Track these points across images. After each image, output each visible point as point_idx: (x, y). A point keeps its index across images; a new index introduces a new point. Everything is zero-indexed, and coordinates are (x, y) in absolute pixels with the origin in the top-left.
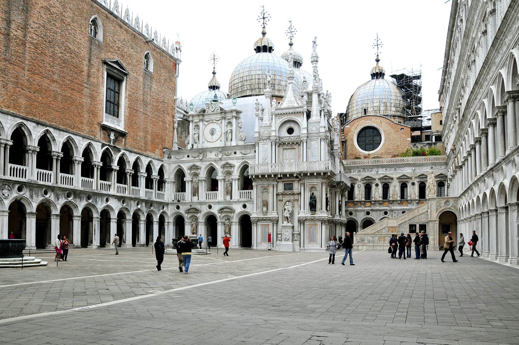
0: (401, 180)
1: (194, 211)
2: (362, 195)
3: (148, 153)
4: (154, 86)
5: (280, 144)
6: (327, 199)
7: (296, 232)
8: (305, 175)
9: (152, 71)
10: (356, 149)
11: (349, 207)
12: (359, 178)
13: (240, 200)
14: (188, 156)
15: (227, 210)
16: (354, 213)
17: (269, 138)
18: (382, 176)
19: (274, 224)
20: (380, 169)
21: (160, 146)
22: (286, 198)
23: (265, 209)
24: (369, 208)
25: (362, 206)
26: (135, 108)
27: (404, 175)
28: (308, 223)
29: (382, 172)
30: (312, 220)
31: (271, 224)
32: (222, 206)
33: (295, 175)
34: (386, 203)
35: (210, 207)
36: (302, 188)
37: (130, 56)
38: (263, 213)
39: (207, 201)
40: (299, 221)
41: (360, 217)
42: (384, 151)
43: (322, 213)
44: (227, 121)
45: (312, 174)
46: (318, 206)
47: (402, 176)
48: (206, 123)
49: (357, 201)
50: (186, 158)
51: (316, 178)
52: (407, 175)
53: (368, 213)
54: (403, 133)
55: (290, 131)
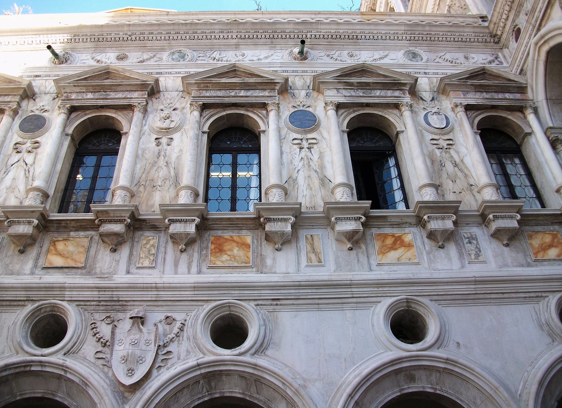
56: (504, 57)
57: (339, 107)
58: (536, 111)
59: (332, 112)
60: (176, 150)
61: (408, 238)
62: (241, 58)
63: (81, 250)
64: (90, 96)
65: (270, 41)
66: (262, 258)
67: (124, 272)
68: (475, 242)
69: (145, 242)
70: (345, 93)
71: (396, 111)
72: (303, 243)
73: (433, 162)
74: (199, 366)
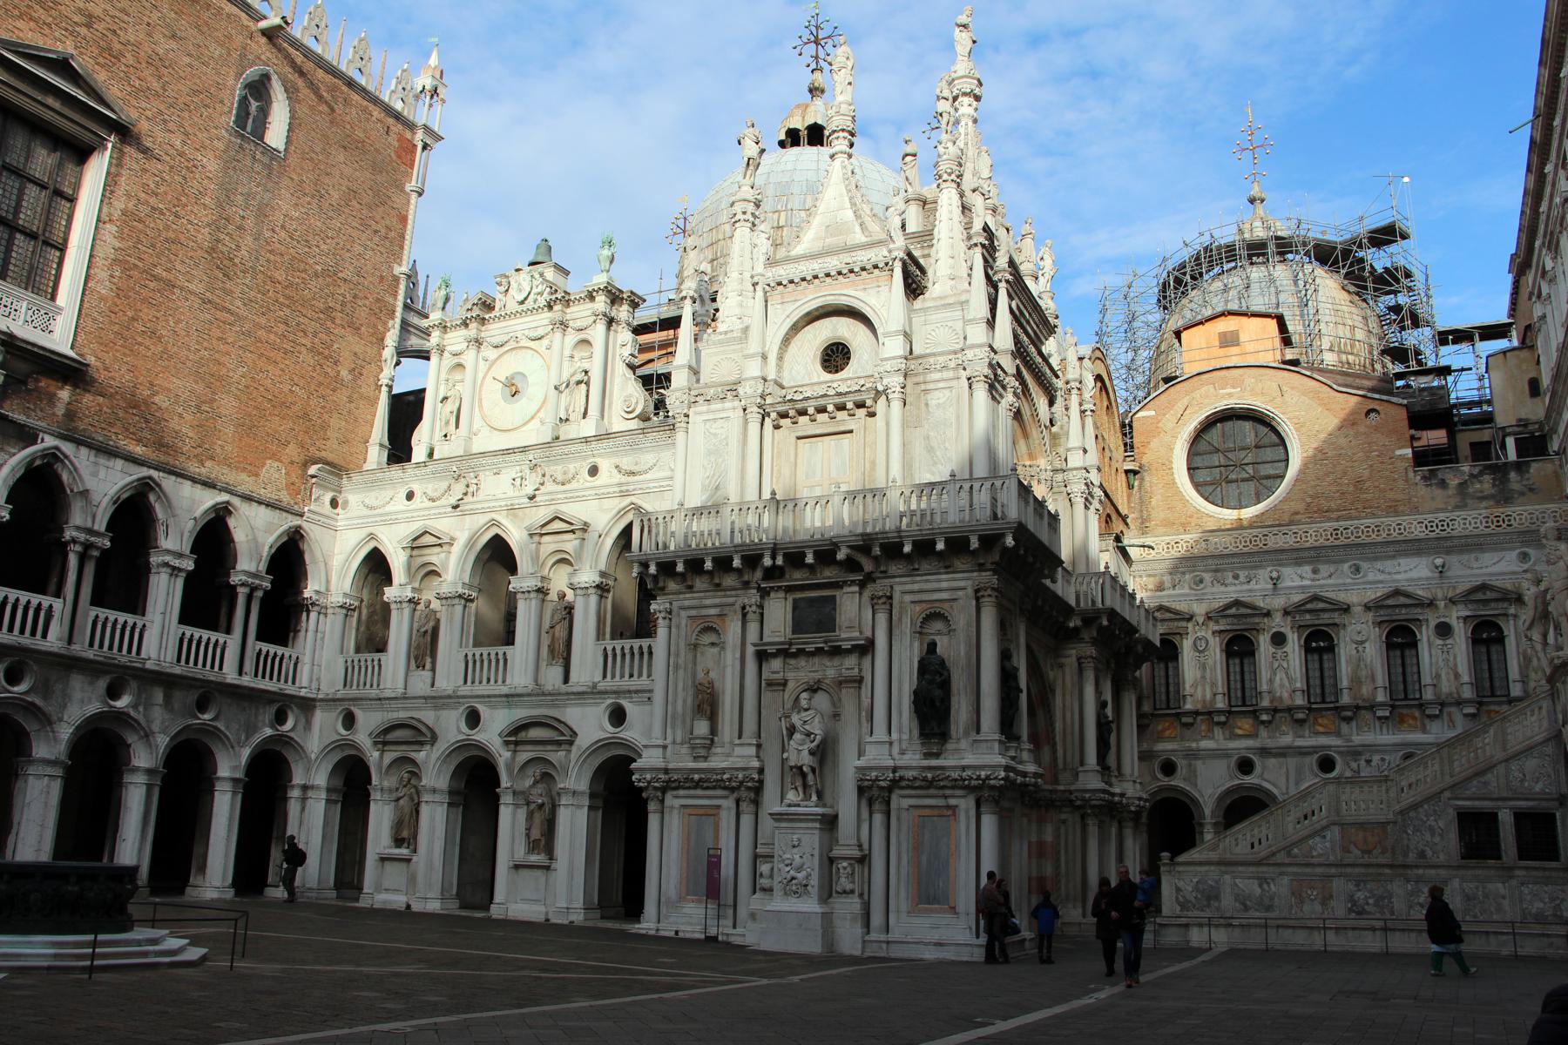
0: (1384, 614)
1: (407, 734)
2: (1213, 685)
3: (208, 470)
4: (285, 205)
5: (786, 411)
6: (1007, 677)
7: (846, 846)
8: (892, 550)
9: (282, 147)
10: (1184, 502)
11: (1160, 738)
12: (1199, 609)
13: (602, 686)
14: (410, 496)
15: (539, 732)
16: (1181, 763)
17: (732, 389)
18: (1297, 598)
19: (743, 806)
20: (1288, 572)
21: (292, 451)
22: (801, 672)
23: (702, 728)
24: (1250, 743)
25: (1217, 731)
26: (158, 271)
27: (1397, 593)
28: (906, 803)
29: (1297, 581)
30: (929, 784)
31: (728, 804)
32: (520, 713)
33: (841, 556)
34: (1326, 721)
35: (473, 719)
36: (882, 618)
37: (157, 63)
38: (693, 748)
39: (466, 690)
40: (861, 790)
41: (1209, 783)
42: (1301, 507)
43: (978, 752)
44: (572, 338)
45: (924, 548)
46: (961, 710)
48: (492, 354)
49: (1197, 713)
50: (400, 503)
51: (949, 568)
52: (1410, 589)
53: (1245, 766)
54: (1376, 429)
55: (835, 356)
57: (1466, 618)
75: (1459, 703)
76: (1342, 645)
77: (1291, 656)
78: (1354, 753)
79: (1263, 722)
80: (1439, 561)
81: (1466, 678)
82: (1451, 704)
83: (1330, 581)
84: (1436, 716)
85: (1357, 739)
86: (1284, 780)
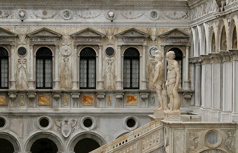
0: (80, 41)
18: (34, 29)
27: (88, 30)
34: (46, 99)
47: (83, 32)
56: (190, 14)
57: (122, 46)
58: (190, 47)
59: (119, 50)
60: (70, 64)
61: (135, 97)
62: (89, 15)
63: (48, 100)
64: (39, 40)
65: (100, 7)
66: (96, 103)
67: (61, 107)
68: (154, 99)
69: (65, 97)
70: (125, 40)
71: (141, 47)
72: (107, 98)
73: (148, 69)
74: (82, 133)
75: (115, 92)
76: (57, 57)
77: (28, 61)
78: (59, 117)
79: (11, 98)
80: (111, 14)
81: (119, 79)
82: (110, 92)
83: (53, 20)
84: (102, 98)
85: (62, 109)
86: (21, 131)
